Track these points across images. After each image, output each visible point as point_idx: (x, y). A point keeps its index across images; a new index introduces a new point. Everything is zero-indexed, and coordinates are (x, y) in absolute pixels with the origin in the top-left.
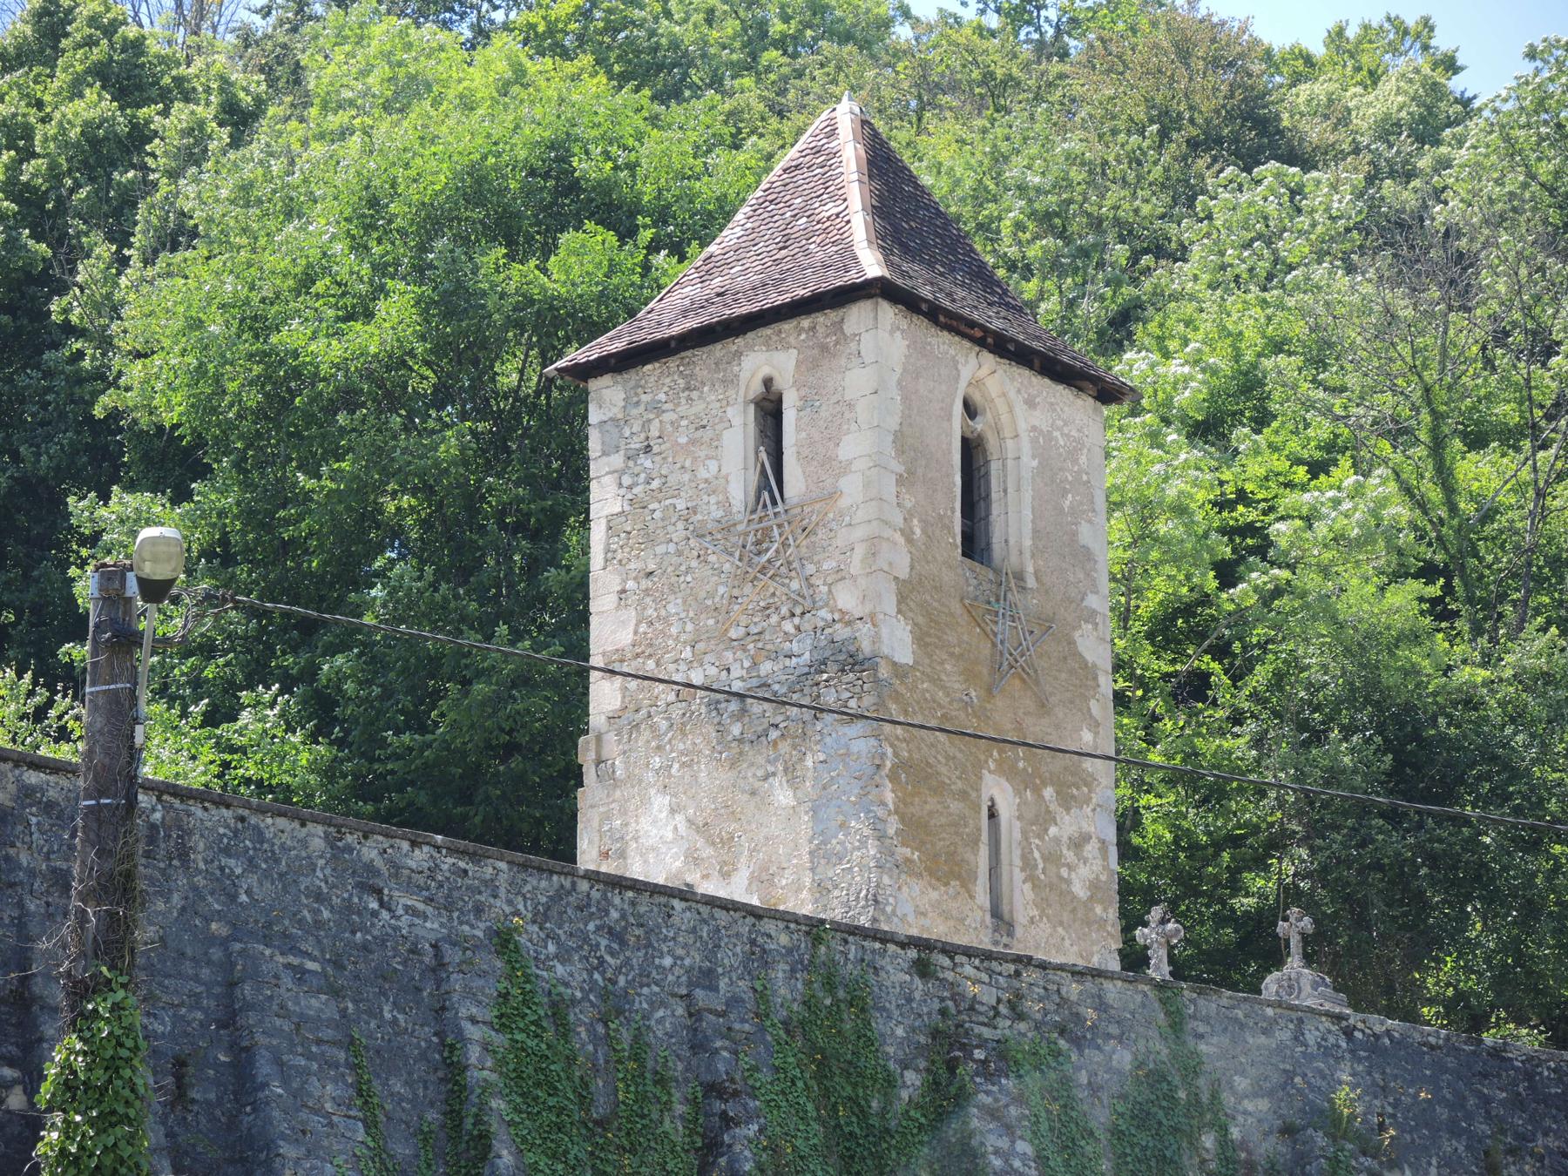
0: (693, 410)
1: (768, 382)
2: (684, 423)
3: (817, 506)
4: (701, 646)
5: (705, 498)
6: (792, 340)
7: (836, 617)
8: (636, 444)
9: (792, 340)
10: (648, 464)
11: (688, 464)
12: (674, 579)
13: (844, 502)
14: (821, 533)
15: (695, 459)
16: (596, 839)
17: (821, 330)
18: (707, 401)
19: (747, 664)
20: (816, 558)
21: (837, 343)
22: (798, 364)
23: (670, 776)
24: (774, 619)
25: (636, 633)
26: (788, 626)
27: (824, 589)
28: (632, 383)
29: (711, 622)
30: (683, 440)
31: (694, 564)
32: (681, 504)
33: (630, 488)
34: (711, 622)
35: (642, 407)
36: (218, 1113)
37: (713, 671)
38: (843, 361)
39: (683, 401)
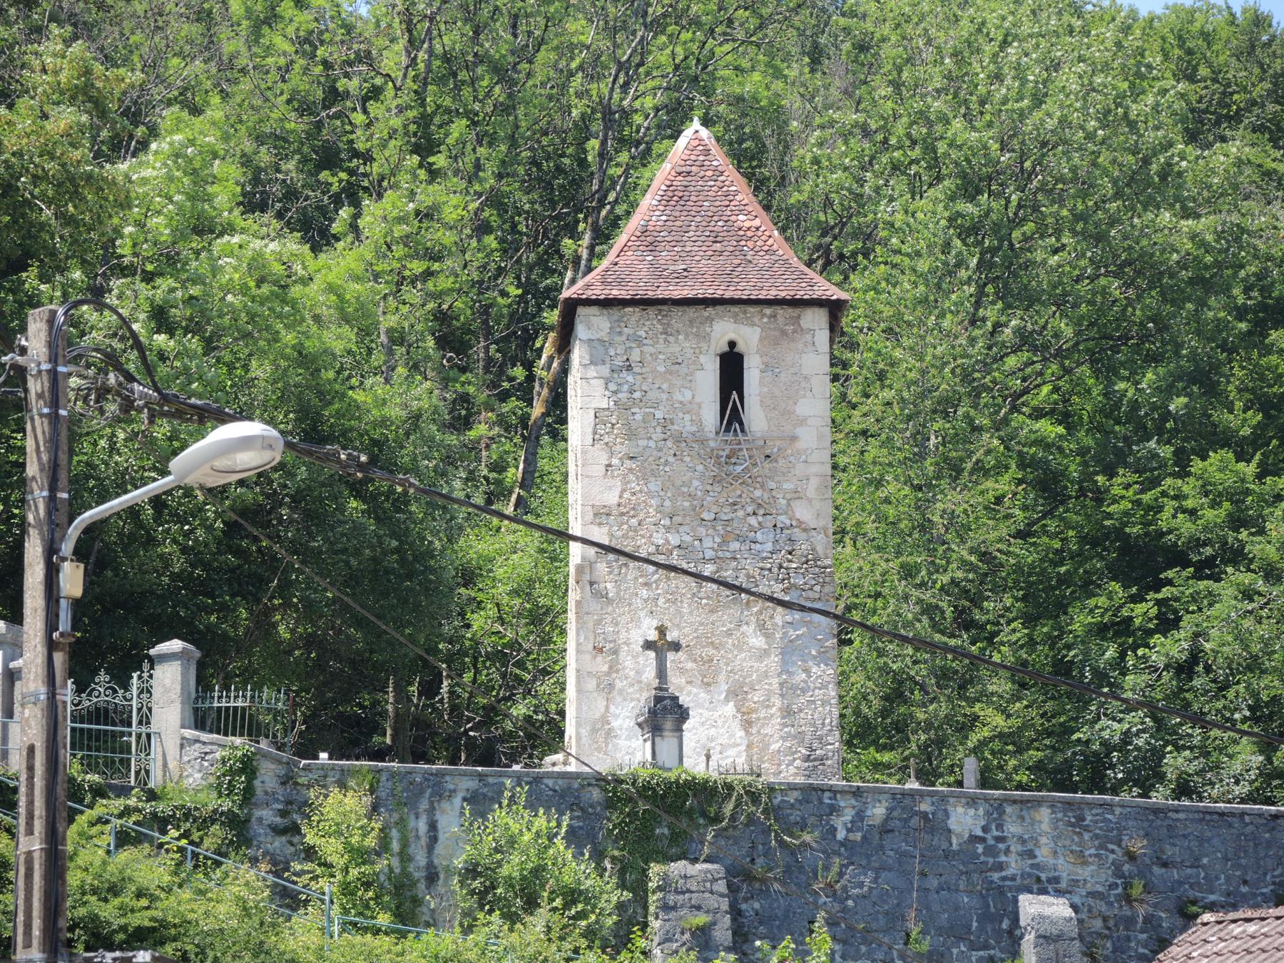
0: (670, 350)
1: (732, 344)
2: (661, 356)
3: (778, 443)
4: (677, 519)
5: (681, 415)
6: (756, 320)
7: (794, 523)
8: (619, 362)
9: (756, 320)
10: (630, 379)
11: (665, 386)
12: (655, 467)
13: (800, 445)
14: (781, 462)
15: (671, 385)
16: (592, 637)
17: (781, 320)
18: (682, 345)
19: (718, 540)
20: (777, 479)
21: (794, 331)
22: (761, 340)
23: (657, 605)
24: (741, 513)
25: (621, 497)
26: (753, 521)
27: (784, 502)
28: (616, 317)
29: (687, 504)
30: (661, 369)
31: (671, 459)
32: (659, 415)
33: (615, 392)
34: (687, 504)
35: (624, 338)
36: (1074, 848)
37: (688, 539)
38: (800, 346)
39: (661, 341)
